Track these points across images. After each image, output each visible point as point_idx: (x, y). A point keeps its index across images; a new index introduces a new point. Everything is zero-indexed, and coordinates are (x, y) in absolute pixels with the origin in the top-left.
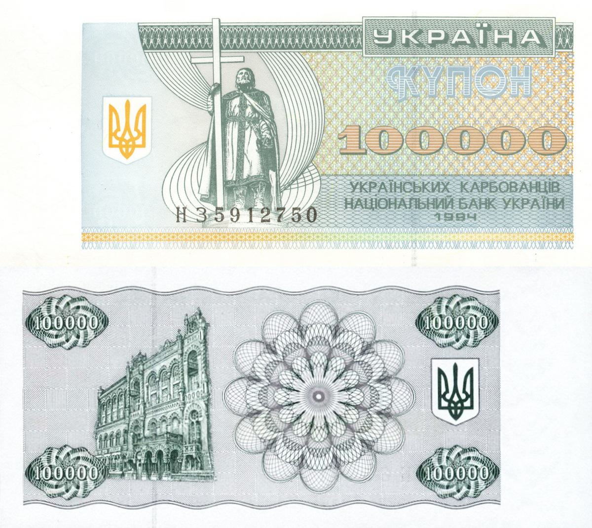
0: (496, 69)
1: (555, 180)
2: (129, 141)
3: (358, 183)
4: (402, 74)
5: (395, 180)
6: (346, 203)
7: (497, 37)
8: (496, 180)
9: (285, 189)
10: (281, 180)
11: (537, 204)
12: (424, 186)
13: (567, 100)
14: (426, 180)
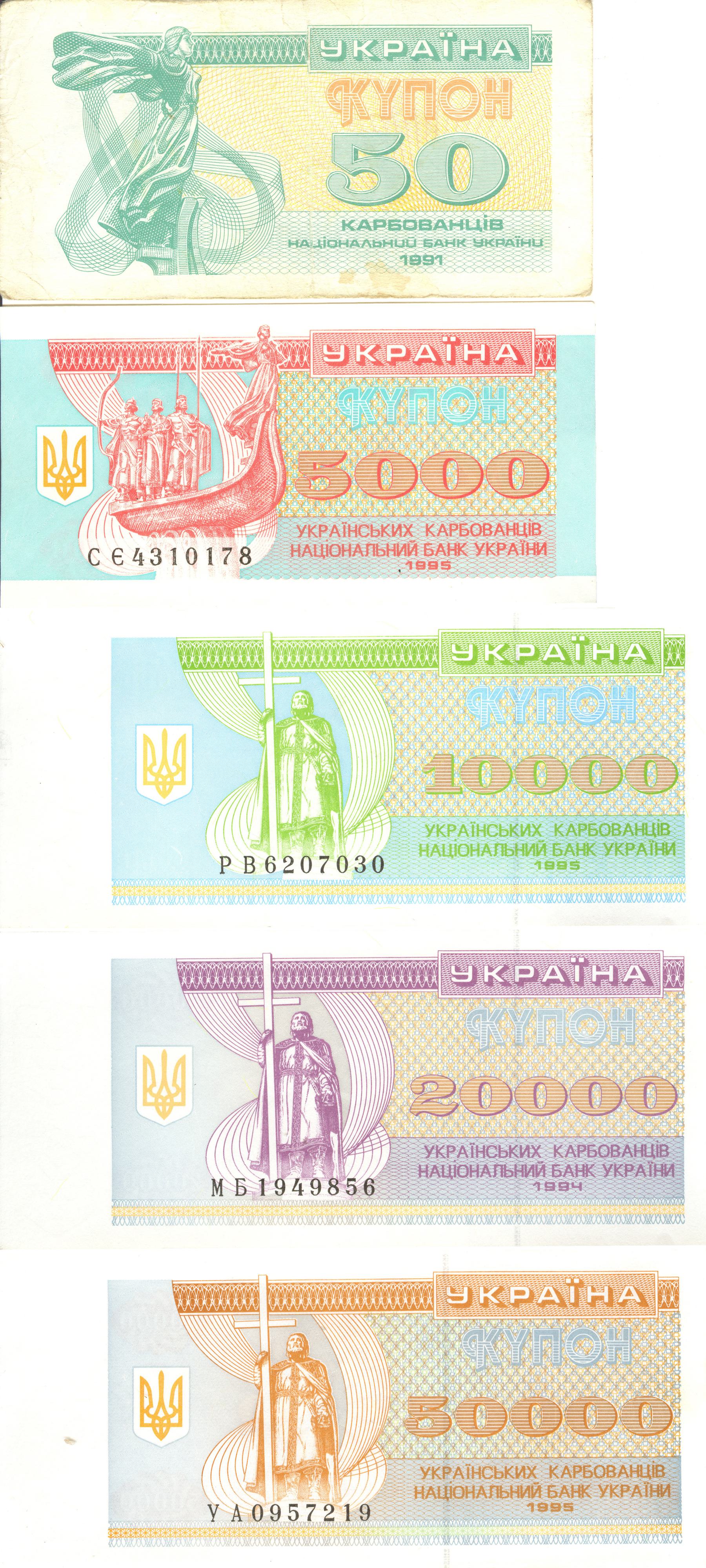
0: (594, 1012)
1: (664, 1143)
2: (167, 1098)
3: (429, 1469)
4: (481, 1339)
5: (477, 1143)
6: (416, 1492)
7: (590, 1294)
8: (591, 1464)
9: (349, 1154)
10: (344, 1144)
11: (639, 1492)
12: (507, 1471)
13: (673, 1367)
14: (512, 1142)
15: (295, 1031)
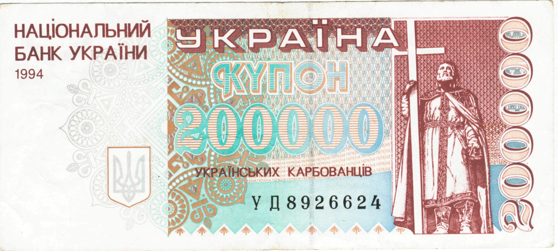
15: (440, 82)
